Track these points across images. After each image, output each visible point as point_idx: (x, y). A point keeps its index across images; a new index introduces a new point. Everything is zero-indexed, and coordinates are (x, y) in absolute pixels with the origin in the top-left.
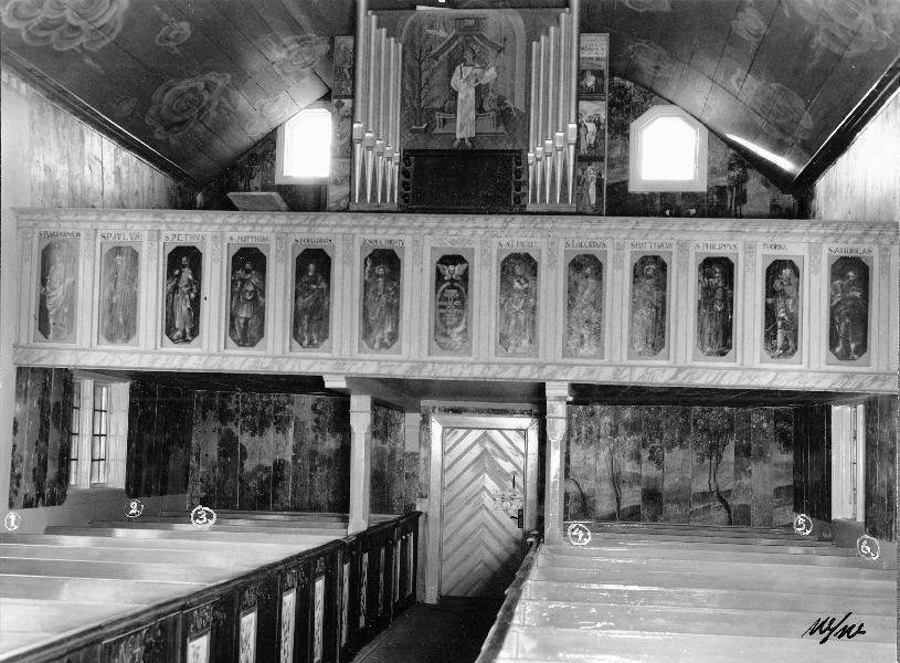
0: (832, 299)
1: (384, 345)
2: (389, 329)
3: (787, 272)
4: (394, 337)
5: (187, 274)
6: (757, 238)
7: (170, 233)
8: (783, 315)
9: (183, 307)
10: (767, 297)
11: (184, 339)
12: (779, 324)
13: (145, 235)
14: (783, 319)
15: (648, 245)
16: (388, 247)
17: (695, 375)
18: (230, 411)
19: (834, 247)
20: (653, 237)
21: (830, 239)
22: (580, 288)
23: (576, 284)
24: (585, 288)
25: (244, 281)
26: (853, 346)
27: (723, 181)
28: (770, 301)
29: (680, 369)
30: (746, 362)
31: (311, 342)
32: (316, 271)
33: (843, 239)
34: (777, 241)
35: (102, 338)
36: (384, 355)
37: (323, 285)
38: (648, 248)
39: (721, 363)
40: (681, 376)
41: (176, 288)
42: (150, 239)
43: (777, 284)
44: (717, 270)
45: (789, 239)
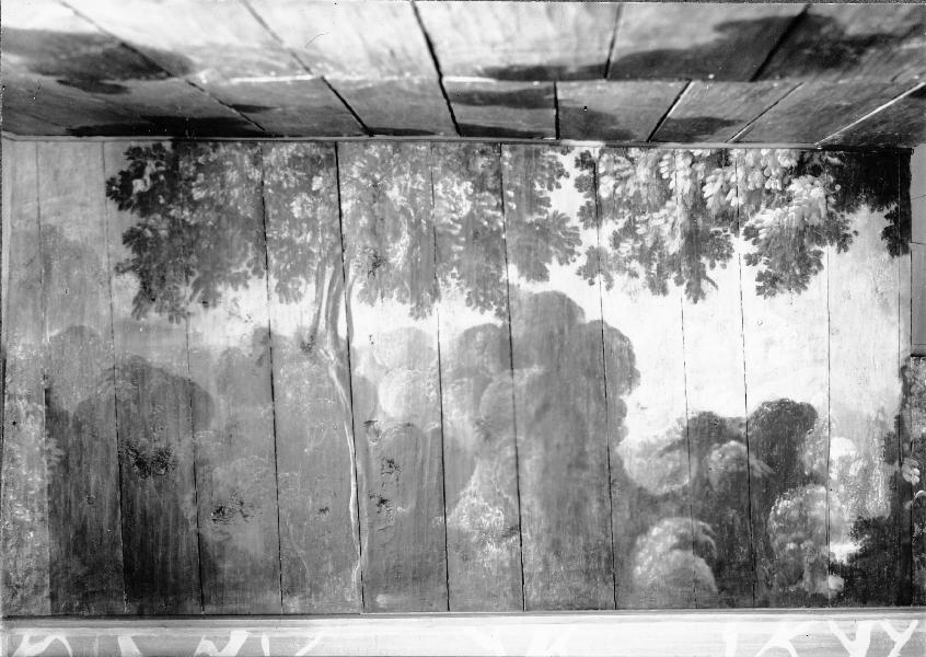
18: (560, 220)
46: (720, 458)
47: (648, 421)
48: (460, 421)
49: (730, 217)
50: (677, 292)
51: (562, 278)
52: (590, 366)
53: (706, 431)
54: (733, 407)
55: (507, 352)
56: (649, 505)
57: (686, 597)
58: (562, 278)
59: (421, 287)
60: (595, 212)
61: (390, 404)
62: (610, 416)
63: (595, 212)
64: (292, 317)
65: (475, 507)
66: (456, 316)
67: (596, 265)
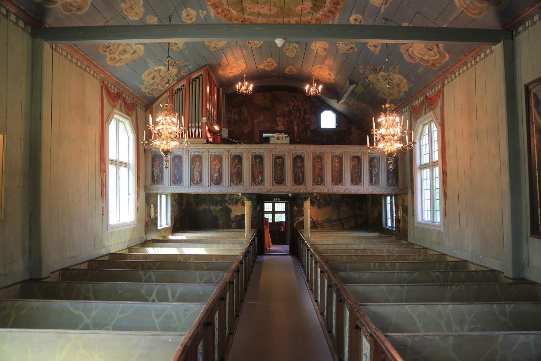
1: (259, 183)
2: (260, 179)
3: (375, 160)
4: (262, 181)
5: (198, 164)
7: (192, 151)
9: (197, 175)
10: (370, 167)
11: (197, 183)
13: (184, 152)
16: (259, 154)
20: (341, 151)
25: (215, 165)
27: (344, 128)
31: (237, 183)
32: (238, 162)
35: (172, 184)
36: (259, 187)
37: (240, 166)
41: (194, 168)
42: (186, 153)
46: (238, 218)
47: (233, 215)
48: (219, 215)
49: (239, 200)
50: (235, 206)
51: (227, 204)
52: (230, 211)
53: (237, 216)
54: (239, 214)
55: (222, 210)
56: (233, 222)
57: (235, 228)
58: (227, 204)
59: (216, 205)
60: (229, 200)
61: (214, 214)
62: (230, 215)
63: (229, 200)
64: (207, 207)
65: (220, 222)
66: (219, 208)
67: (229, 204)
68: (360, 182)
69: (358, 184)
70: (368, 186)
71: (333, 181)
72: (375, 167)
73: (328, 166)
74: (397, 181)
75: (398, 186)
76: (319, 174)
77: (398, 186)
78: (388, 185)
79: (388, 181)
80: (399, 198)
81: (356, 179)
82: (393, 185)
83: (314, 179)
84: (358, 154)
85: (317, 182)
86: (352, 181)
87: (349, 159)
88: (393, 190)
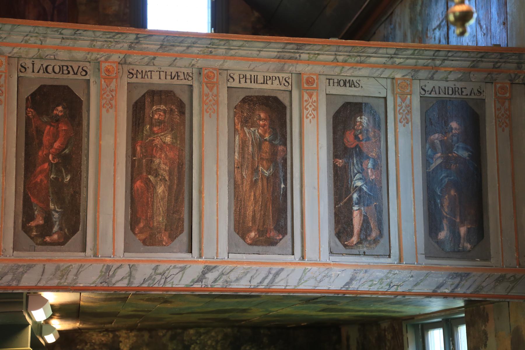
0: (427, 161)
3: (364, 120)
6: (318, 69)
8: (359, 184)
10: (336, 156)
12: (355, 196)
14: (360, 189)
15: (155, 76)
17: (233, 276)
19: (429, 85)
21: (423, 74)
22: (46, 139)
23: (40, 132)
24: (55, 137)
26: (463, 230)
28: (340, 162)
29: (208, 269)
30: (309, 254)
33: (440, 75)
34: (348, 73)
38: (155, 79)
39: (271, 257)
40: (211, 276)
43: (349, 139)
44: (262, 115)
45: (365, 72)
68: (282, 229)
69: (273, 243)
70: (325, 257)
71: (133, 222)
72: (360, 154)
73: (108, 141)
74: (480, 231)
75: (487, 258)
76: (58, 187)
77: (487, 258)
78: (434, 248)
79: (432, 225)
80: (490, 328)
81: (266, 220)
82: (458, 253)
83: (27, 214)
84: (272, 87)
85: (46, 229)
86: (240, 228)
87: (224, 111)
88: (464, 276)
